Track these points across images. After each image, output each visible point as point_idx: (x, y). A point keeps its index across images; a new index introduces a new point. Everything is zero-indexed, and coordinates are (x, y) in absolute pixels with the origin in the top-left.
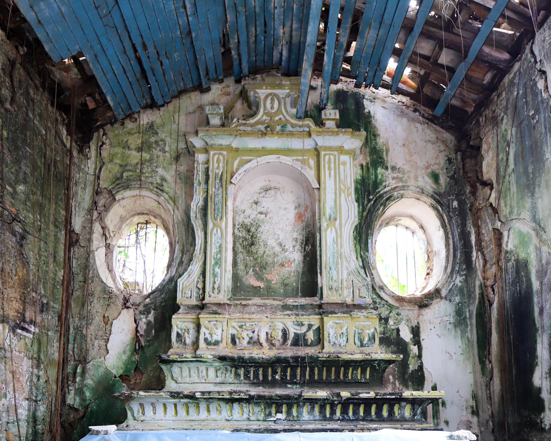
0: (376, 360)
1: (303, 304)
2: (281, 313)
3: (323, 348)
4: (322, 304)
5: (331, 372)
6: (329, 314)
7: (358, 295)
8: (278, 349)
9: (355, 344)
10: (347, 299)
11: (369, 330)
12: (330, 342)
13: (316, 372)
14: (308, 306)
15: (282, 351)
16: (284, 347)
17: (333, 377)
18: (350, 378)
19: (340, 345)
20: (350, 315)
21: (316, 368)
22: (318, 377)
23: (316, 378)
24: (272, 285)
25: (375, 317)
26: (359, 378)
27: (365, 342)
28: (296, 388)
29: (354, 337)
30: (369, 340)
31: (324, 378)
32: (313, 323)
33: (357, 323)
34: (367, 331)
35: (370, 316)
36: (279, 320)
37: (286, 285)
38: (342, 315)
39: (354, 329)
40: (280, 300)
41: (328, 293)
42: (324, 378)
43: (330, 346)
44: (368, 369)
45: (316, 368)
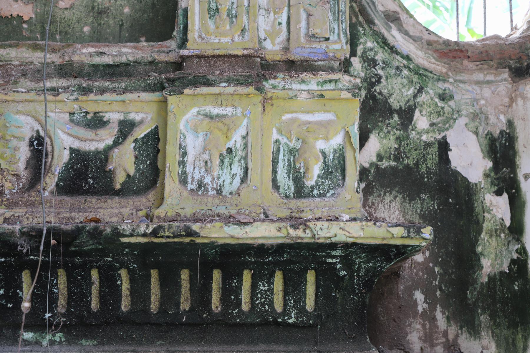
0: (333, 246)
1: (124, 59)
2: (33, 85)
3: (161, 200)
4: (183, 58)
5: (178, 284)
6: (186, 86)
7: (303, 31)
8: (11, 205)
9: (276, 186)
10: (268, 45)
11: (327, 139)
12: (183, 181)
13: (125, 286)
14: (141, 69)
15: (18, 212)
16: (33, 196)
17: (185, 305)
18: (245, 307)
19: (219, 192)
20: (260, 89)
21: (123, 272)
22: (133, 303)
23: (125, 305)
24: (59, 13)
25: (346, 95)
26: (279, 307)
27: (310, 182)
28: (52, 343)
29: (275, 162)
30: (327, 173)
31: (154, 306)
32: (136, 117)
33: (287, 117)
34: (320, 145)
35: (327, 95)
36: (20, 107)
37: (102, 12)
38: (231, 90)
39: (275, 135)
40: (54, 51)
41: (203, 25)
42: (154, 306)
43: (186, 194)
44: (311, 277)
45: (123, 272)
